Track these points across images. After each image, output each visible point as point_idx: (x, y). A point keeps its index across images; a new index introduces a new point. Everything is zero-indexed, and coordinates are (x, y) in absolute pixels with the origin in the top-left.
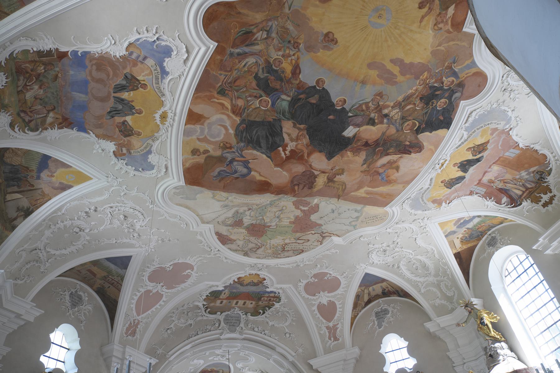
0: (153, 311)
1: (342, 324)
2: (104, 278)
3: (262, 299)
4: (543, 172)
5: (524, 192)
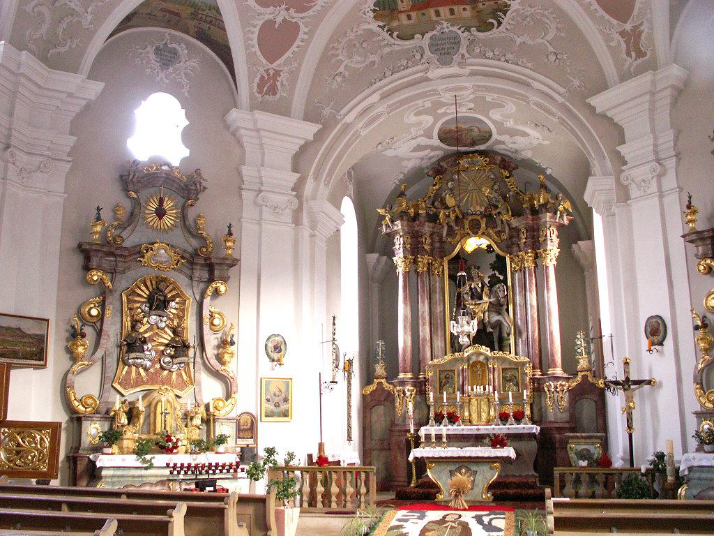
0: (294, 52)
1: (650, 22)
2: (194, 16)
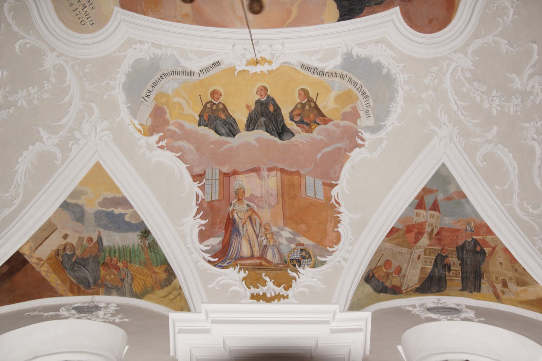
4: (310, 256)
5: (252, 257)
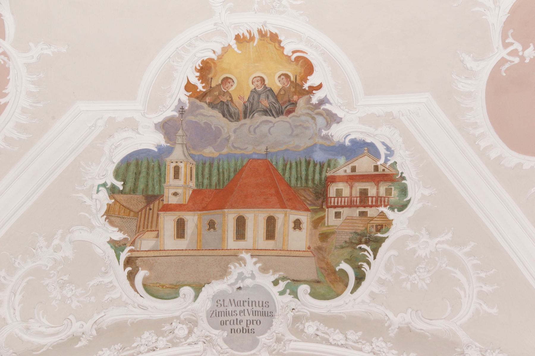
3: (332, 191)
